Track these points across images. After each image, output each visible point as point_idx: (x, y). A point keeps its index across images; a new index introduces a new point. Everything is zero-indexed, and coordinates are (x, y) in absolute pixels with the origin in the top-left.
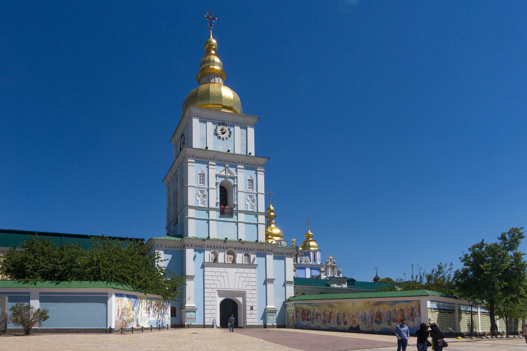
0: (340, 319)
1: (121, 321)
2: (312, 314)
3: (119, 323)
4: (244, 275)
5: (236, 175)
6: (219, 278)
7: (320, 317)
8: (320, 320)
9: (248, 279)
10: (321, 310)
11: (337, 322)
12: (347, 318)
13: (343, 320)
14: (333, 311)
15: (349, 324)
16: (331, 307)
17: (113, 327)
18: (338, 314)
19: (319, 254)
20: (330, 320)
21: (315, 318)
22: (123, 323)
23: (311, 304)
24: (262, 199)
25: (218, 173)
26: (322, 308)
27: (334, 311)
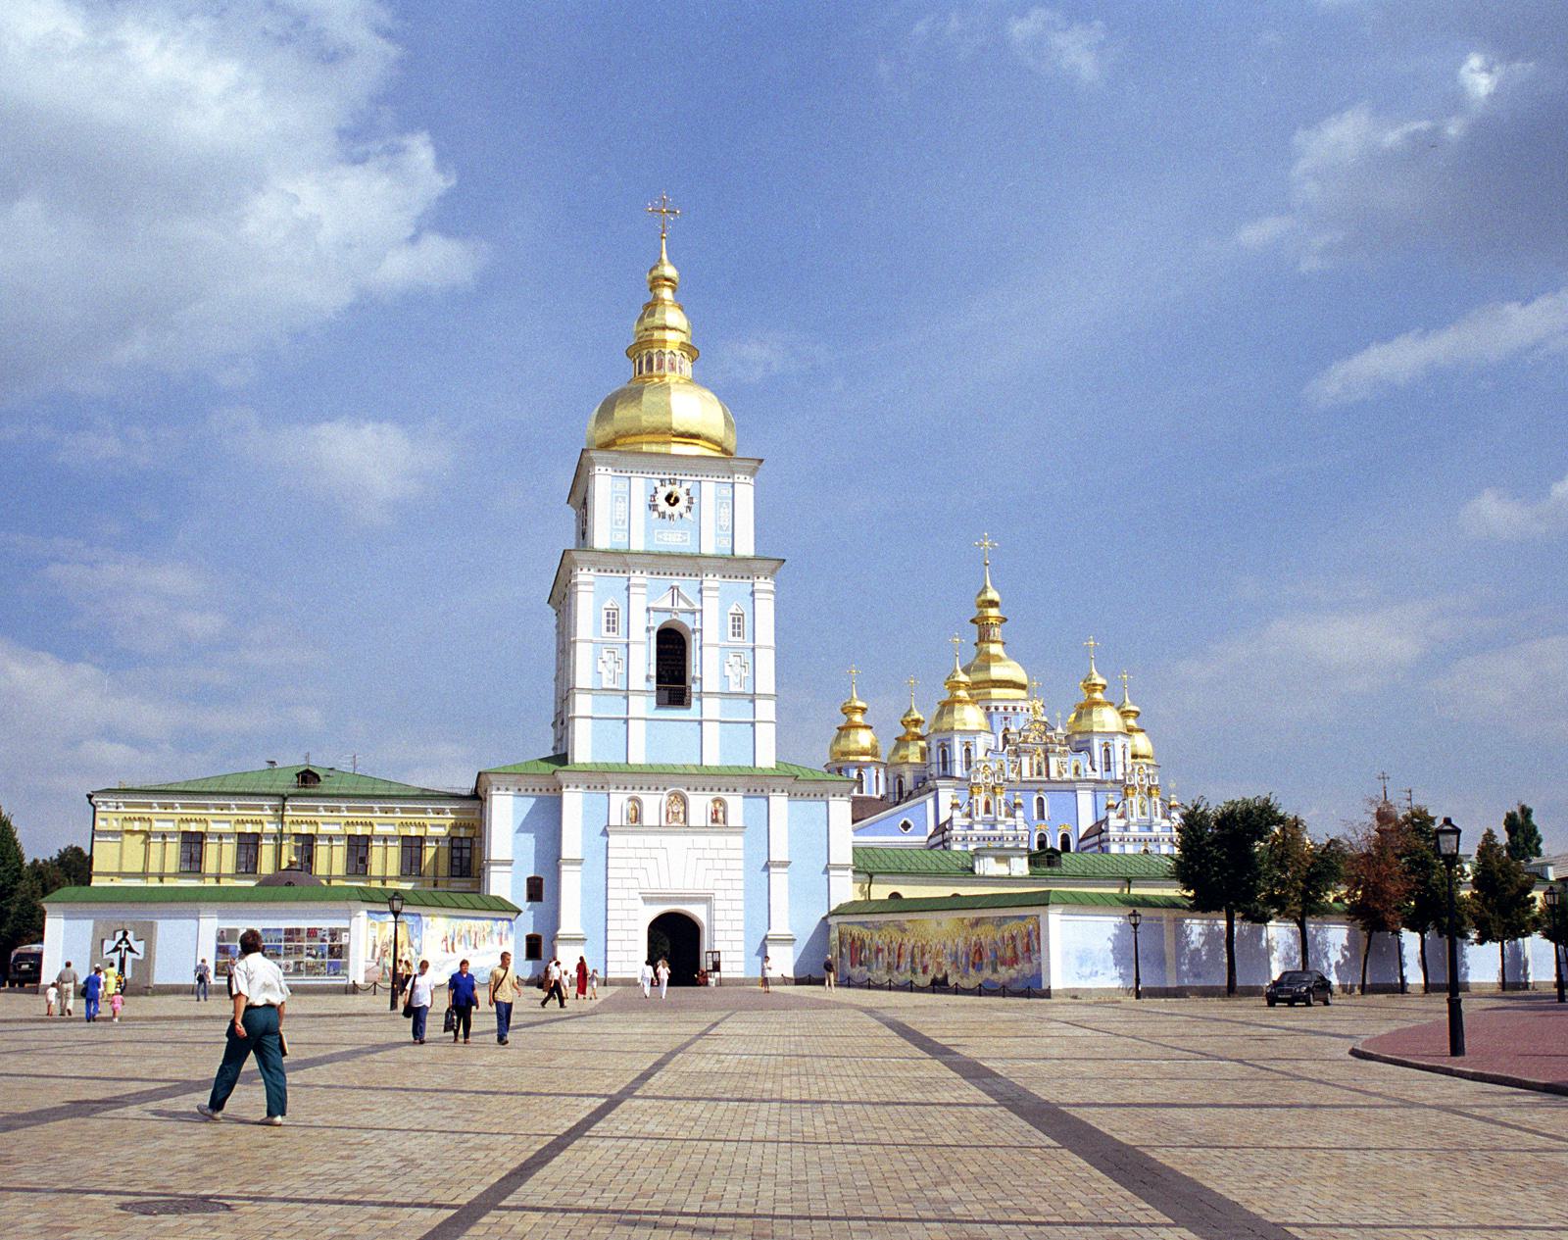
0: (917, 960)
1: (380, 968)
3: (374, 973)
4: (708, 854)
5: (697, 606)
6: (645, 863)
9: (720, 864)
11: (911, 967)
12: (927, 956)
13: (922, 962)
15: (932, 972)
17: (360, 981)
18: (914, 947)
19: (1124, 746)
22: (384, 973)
24: (766, 662)
25: (651, 605)
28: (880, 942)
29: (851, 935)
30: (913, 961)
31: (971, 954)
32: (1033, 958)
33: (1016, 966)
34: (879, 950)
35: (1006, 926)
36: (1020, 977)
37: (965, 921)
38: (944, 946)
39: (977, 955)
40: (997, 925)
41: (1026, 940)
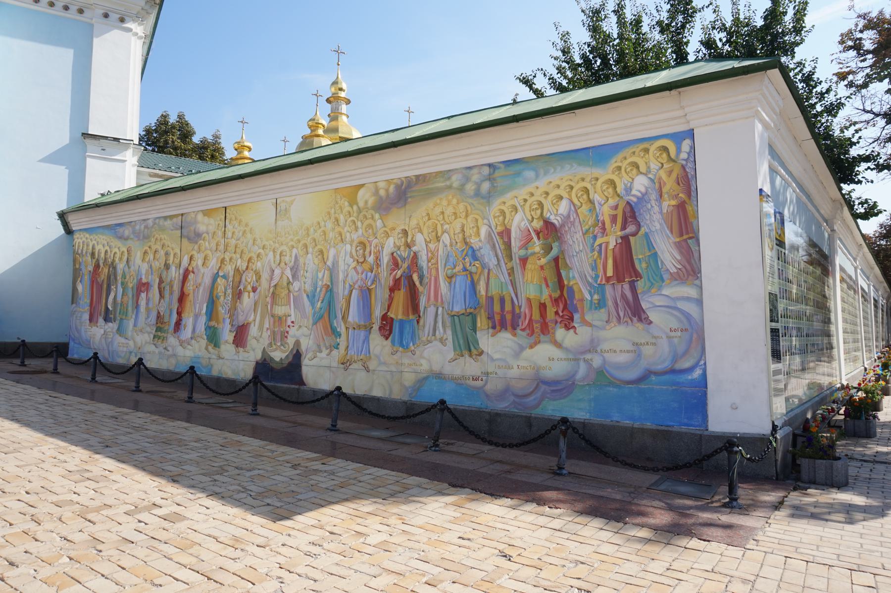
0: (222, 311)
2: (122, 284)
7: (148, 300)
8: (146, 319)
10: (151, 256)
11: (208, 328)
12: (247, 300)
14: (194, 264)
16: (189, 239)
20: (179, 314)
21: (130, 303)
23: (120, 230)
26: (158, 246)
27: (200, 263)
28: (145, 267)
29: (93, 254)
30: (212, 313)
31: (380, 296)
32: (644, 305)
33: (560, 333)
34: (142, 287)
35: (523, 193)
36: (582, 370)
37: (361, 192)
38: (295, 276)
39: (401, 296)
40: (477, 194)
41: (612, 240)
